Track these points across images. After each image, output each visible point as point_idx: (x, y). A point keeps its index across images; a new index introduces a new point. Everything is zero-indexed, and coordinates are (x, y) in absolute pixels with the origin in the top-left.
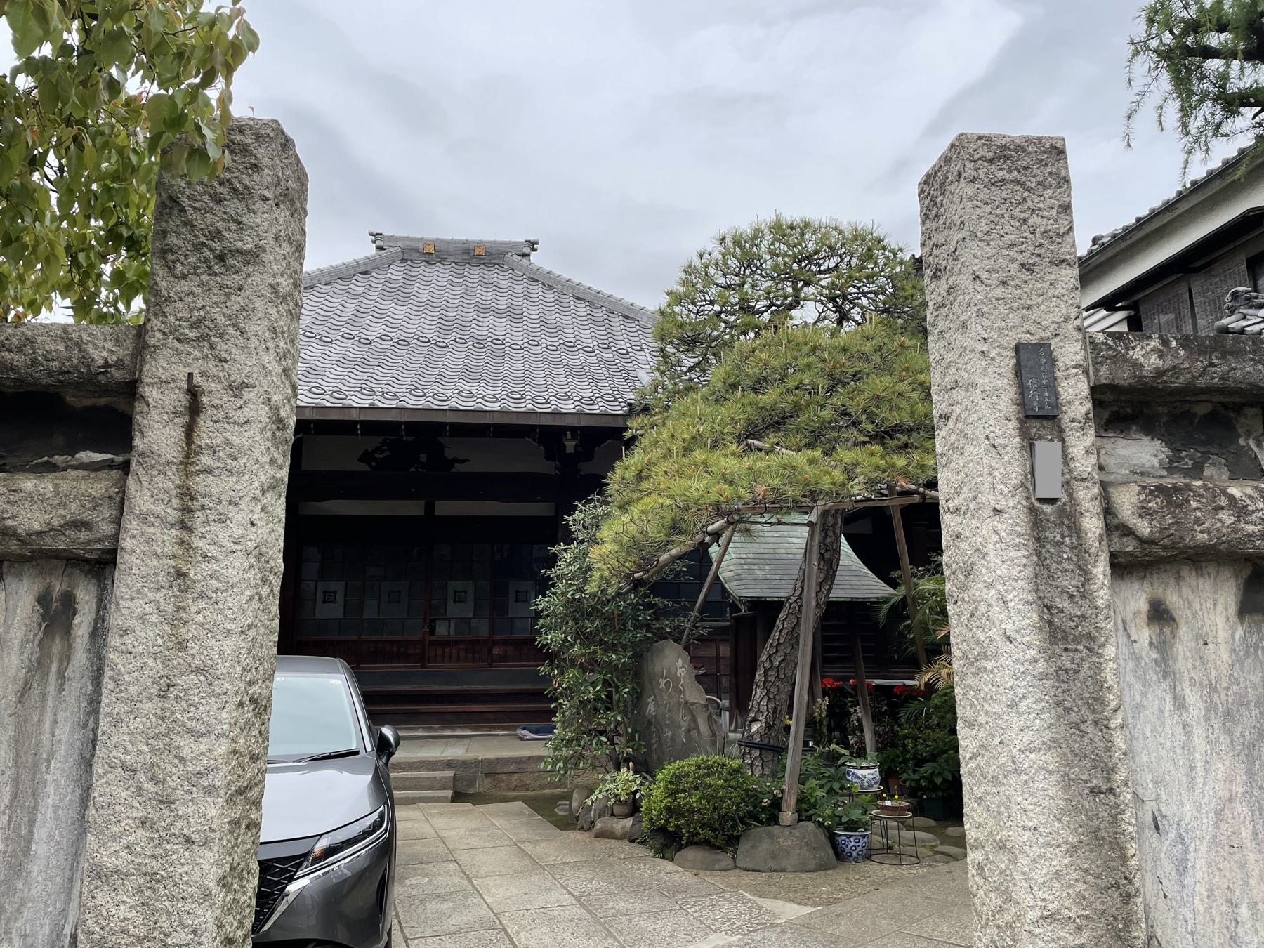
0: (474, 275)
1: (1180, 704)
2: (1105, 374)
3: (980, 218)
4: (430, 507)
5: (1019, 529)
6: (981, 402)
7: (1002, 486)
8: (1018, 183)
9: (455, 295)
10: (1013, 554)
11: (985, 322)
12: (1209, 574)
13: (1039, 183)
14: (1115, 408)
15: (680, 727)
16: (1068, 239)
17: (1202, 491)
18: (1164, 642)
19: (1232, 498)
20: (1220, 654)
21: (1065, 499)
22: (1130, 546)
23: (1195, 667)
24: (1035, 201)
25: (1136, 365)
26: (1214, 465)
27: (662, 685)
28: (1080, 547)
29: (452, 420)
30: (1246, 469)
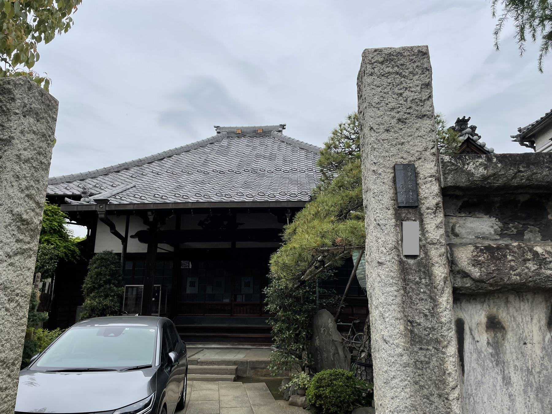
0: (257, 141)
1: (507, 381)
2: (450, 180)
3: (374, 95)
4: (233, 245)
5: (392, 274)
6: (373, 199)
7: (383, 249)
8: (397, 73)
9: (247, 150)
10: (388, 289)
11: (376, 153)
12: (528, 300)
13: (410, 73)
14: (466, 199)
15: (330, 352)
16: (428, 103)
17: (516, 249)
18: (497, 342)
19: (536, 254)
20: (535, 351)
21: (422, 255)
22: (468, 284)
23: (518, 359)
24: (408, 83)
25: (470, 174)
26: (531, 232)
27: (322, 331)
28: (431, 285)
29: (231, 207)
30: (548, 235)
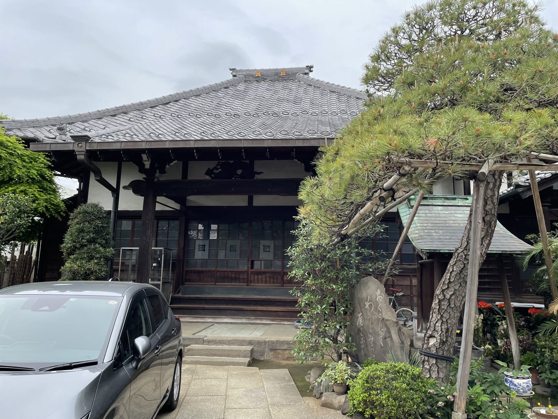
0: (279, 86)
9: (267, 95)
27: (367, 306)
29: (245, 146)
